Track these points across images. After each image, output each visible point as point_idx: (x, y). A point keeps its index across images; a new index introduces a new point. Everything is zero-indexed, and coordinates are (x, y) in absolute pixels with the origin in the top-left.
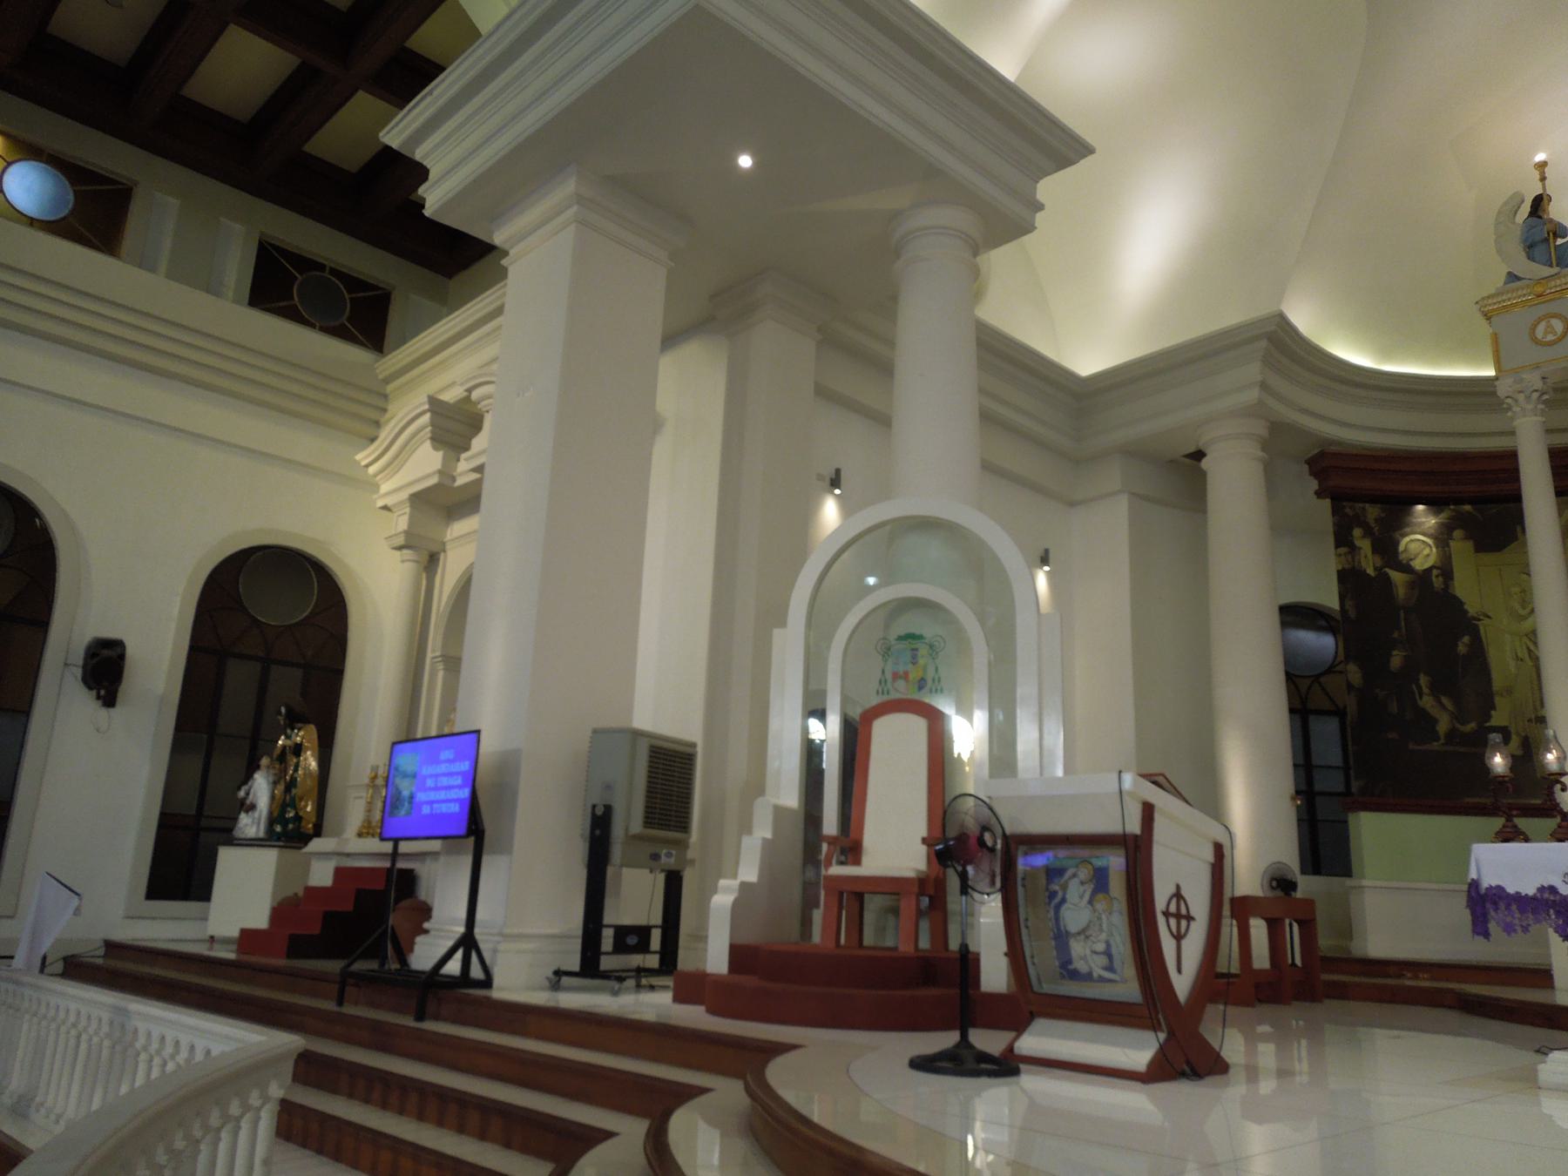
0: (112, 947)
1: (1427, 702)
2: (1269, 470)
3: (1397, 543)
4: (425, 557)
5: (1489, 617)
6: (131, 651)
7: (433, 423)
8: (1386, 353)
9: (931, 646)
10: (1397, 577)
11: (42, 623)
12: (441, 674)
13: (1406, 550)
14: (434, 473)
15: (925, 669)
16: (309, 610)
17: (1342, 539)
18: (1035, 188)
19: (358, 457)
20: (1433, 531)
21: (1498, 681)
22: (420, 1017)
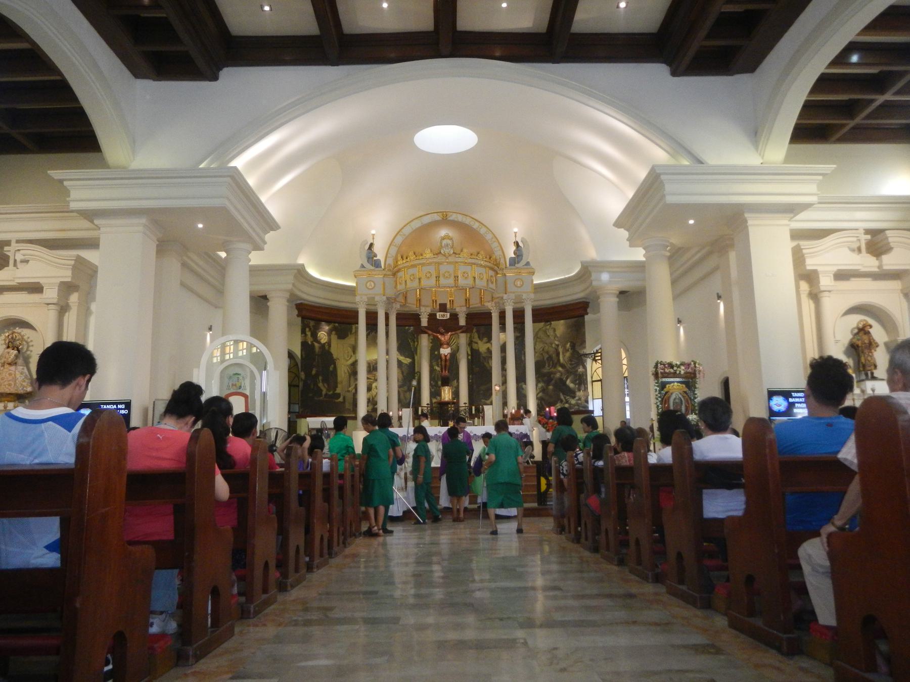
1: (320, 385)
2: (289, 309)
3: (317, 334)
5: (338, 359)
8: (323, 274)
9: (243, 377)
10: (316, 345)
13: (319, 336)
15: (241, 383)
17: (303, 332)
18: (265, 237)
20: (327, 331)
21: (339, 379)
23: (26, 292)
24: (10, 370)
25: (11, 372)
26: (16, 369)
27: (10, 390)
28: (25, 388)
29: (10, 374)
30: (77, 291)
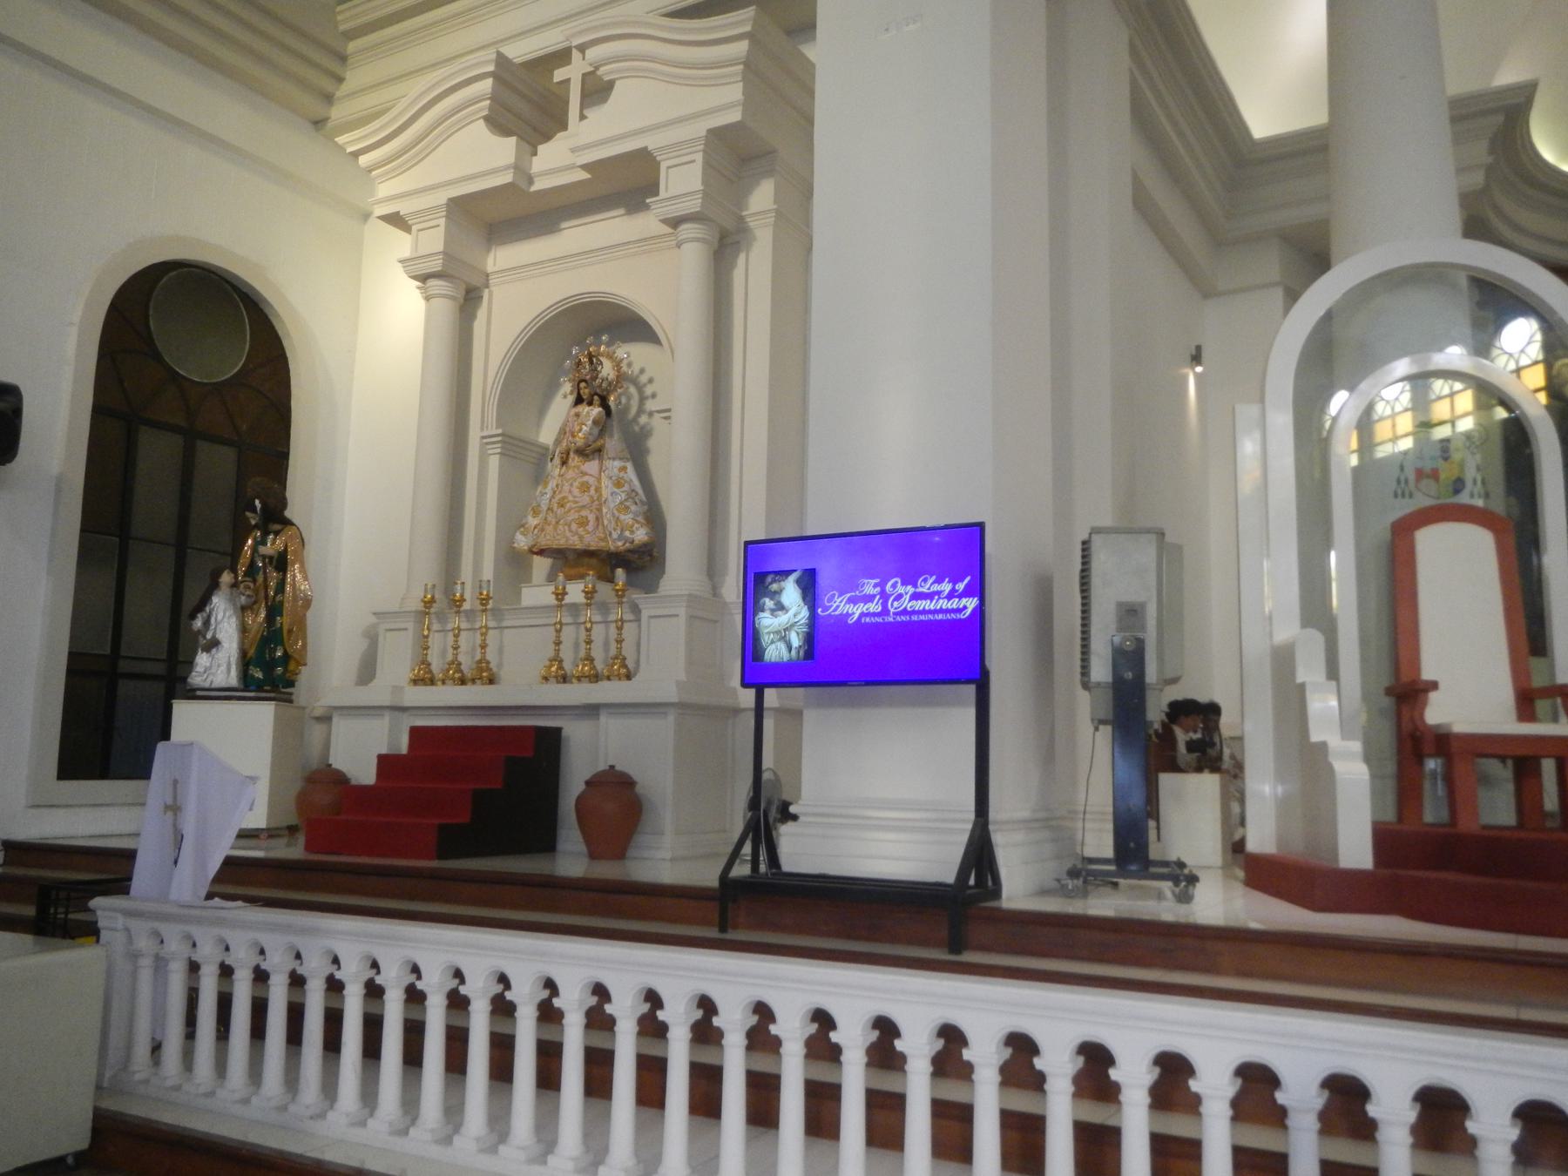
4: (460, 295)
7: (494, 98)
12: (494, 462)
14: (507, 168)
15: (1462, 465)
23: (621, 211)
24: (584, 474)
25: (586, 478)
26: (601, 470)
27: (581, 538)
28: (627, 533)
29: (585, 487)
30: (769, 173)
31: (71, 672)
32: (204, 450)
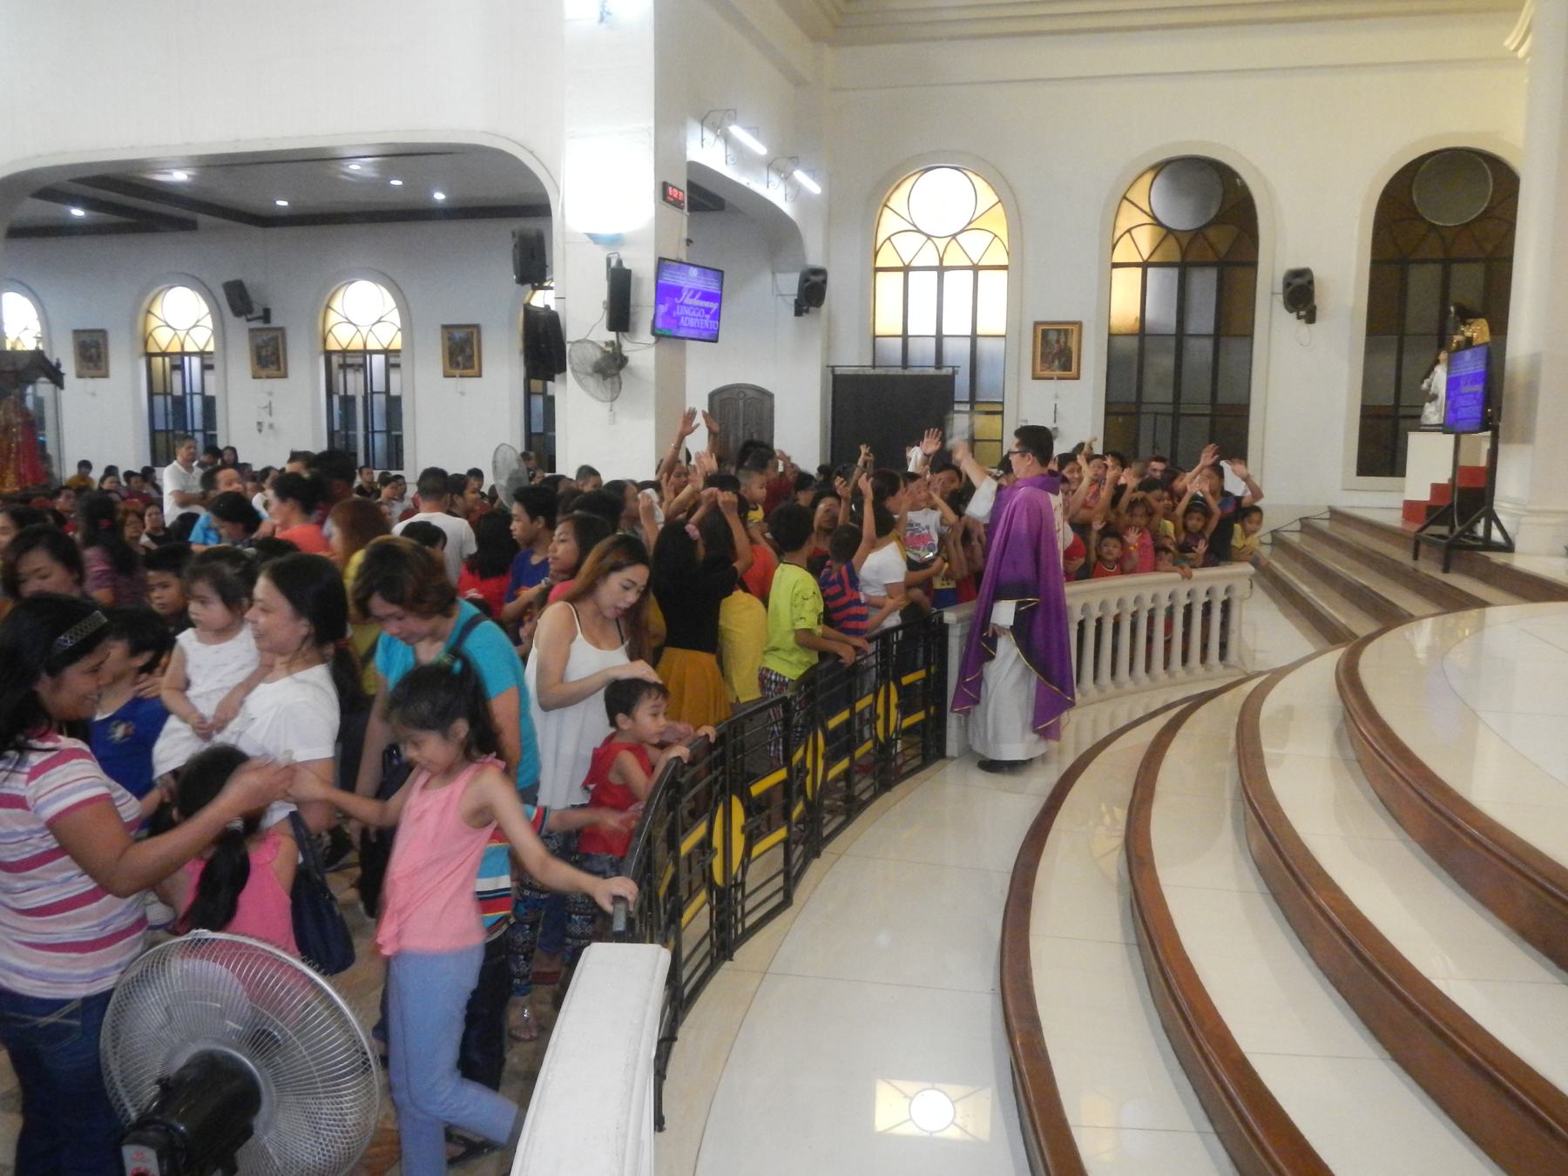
0: (1336, 515)
6: (1318, 274)
11: (1253, 265)
16: (1486, 205)
19: (1507, 43)
22: (1446, 570)
31: (1363, 417)
32: (1458, 271)
